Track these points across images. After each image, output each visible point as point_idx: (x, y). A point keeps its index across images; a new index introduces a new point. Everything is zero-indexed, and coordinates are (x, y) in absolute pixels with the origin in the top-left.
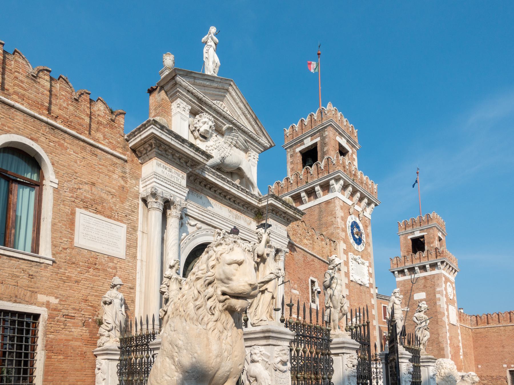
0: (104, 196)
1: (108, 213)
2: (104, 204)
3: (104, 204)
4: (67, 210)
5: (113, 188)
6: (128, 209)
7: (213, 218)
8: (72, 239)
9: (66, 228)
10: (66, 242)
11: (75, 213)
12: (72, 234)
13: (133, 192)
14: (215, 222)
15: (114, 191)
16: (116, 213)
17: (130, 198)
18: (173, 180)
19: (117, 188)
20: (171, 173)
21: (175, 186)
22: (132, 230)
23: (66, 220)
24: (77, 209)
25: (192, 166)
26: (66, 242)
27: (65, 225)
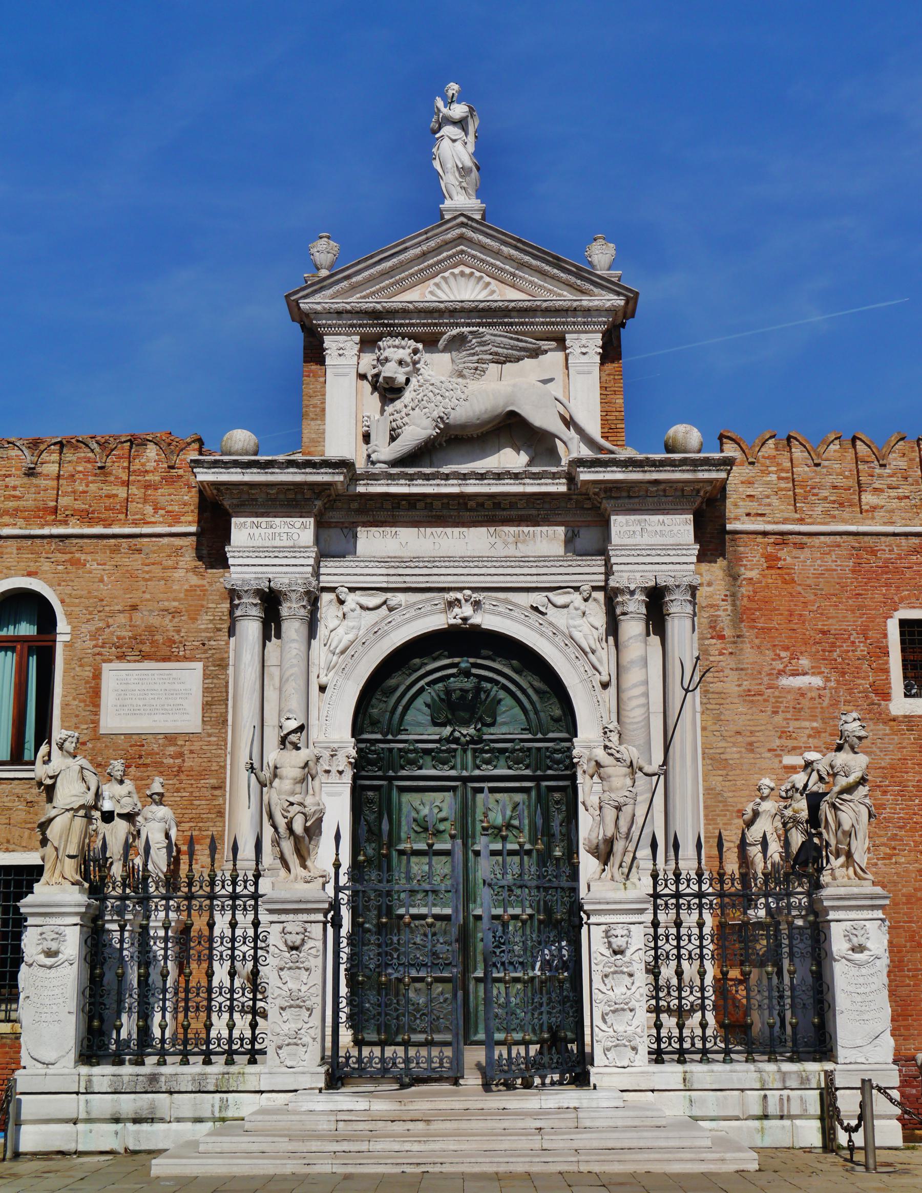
0: (155, 621)
1: (165, 651)
2: (156, 637)
3: (156, 637)
4: (87, 673)
5: (174, 600)
6: (206, 630)
7: (435, 571)
8: (96, 723)
9: (86, 705)
10: (85, 731)
11: (100, 673)
12: (97, 714)
13: (218, 590)
14: (442, 578)
15: (176, 604)
16: (181, 645)
17: (211, 605)
18: (277, 543)
19: (182, 595)
20: (272, 530)
21: (281, 555)
22: (218, 668)
23: (84, 691)
24: (105, 666)
25: (318, 496)
26: (85, 731)
27: (84, 701)
